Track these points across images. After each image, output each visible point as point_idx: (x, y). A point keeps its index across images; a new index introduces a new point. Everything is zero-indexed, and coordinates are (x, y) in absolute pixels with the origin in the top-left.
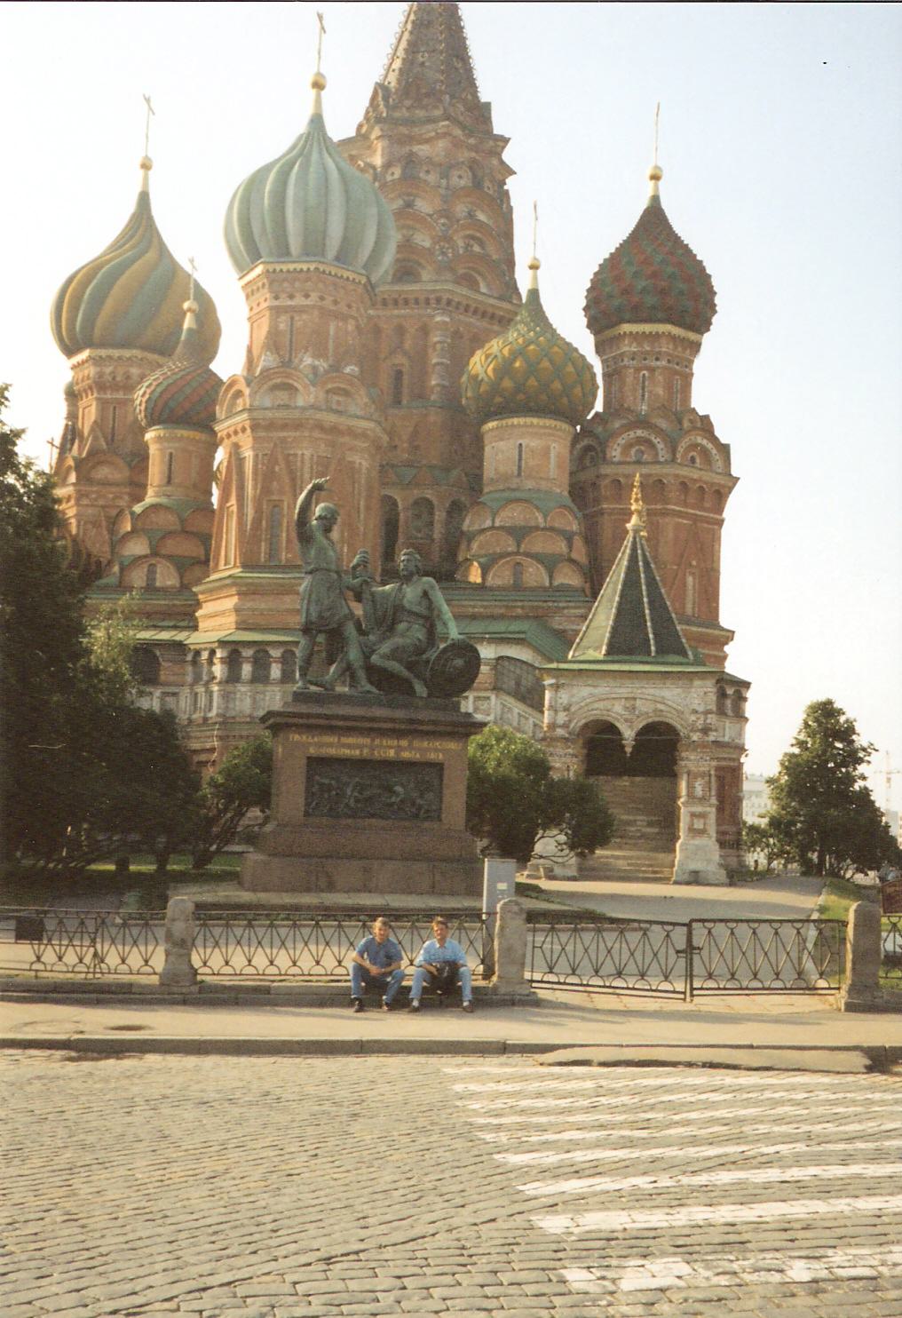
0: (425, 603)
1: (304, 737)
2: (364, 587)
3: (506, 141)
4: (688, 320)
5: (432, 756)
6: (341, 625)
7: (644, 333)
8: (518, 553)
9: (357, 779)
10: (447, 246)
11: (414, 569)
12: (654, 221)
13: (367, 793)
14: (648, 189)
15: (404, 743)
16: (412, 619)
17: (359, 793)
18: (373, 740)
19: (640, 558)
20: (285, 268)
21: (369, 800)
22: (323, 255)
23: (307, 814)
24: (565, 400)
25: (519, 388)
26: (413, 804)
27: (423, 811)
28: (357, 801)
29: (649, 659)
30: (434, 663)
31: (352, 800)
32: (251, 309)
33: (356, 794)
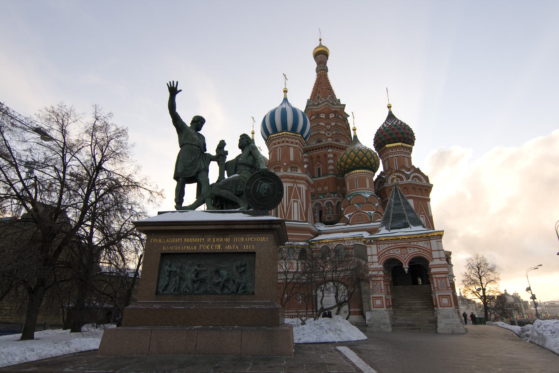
1: (160, 240)
2: (221, 158)
3: (345, 105)
4: (406, 141)
5: (246, 248)
6: (198, 172)
8: (359, 211)
9: (196, 267)
11: (246, 143)
14: (387, 111)
15: (227, 240)
17: (196, 276)
18: (206, 239)
20: (276, 135)
21: (203, 281)
24: (368, 163)
25: (353, 161)
26: (234, 282)
28: (194, 282)
30: (247, 184)
31: (190, 282)
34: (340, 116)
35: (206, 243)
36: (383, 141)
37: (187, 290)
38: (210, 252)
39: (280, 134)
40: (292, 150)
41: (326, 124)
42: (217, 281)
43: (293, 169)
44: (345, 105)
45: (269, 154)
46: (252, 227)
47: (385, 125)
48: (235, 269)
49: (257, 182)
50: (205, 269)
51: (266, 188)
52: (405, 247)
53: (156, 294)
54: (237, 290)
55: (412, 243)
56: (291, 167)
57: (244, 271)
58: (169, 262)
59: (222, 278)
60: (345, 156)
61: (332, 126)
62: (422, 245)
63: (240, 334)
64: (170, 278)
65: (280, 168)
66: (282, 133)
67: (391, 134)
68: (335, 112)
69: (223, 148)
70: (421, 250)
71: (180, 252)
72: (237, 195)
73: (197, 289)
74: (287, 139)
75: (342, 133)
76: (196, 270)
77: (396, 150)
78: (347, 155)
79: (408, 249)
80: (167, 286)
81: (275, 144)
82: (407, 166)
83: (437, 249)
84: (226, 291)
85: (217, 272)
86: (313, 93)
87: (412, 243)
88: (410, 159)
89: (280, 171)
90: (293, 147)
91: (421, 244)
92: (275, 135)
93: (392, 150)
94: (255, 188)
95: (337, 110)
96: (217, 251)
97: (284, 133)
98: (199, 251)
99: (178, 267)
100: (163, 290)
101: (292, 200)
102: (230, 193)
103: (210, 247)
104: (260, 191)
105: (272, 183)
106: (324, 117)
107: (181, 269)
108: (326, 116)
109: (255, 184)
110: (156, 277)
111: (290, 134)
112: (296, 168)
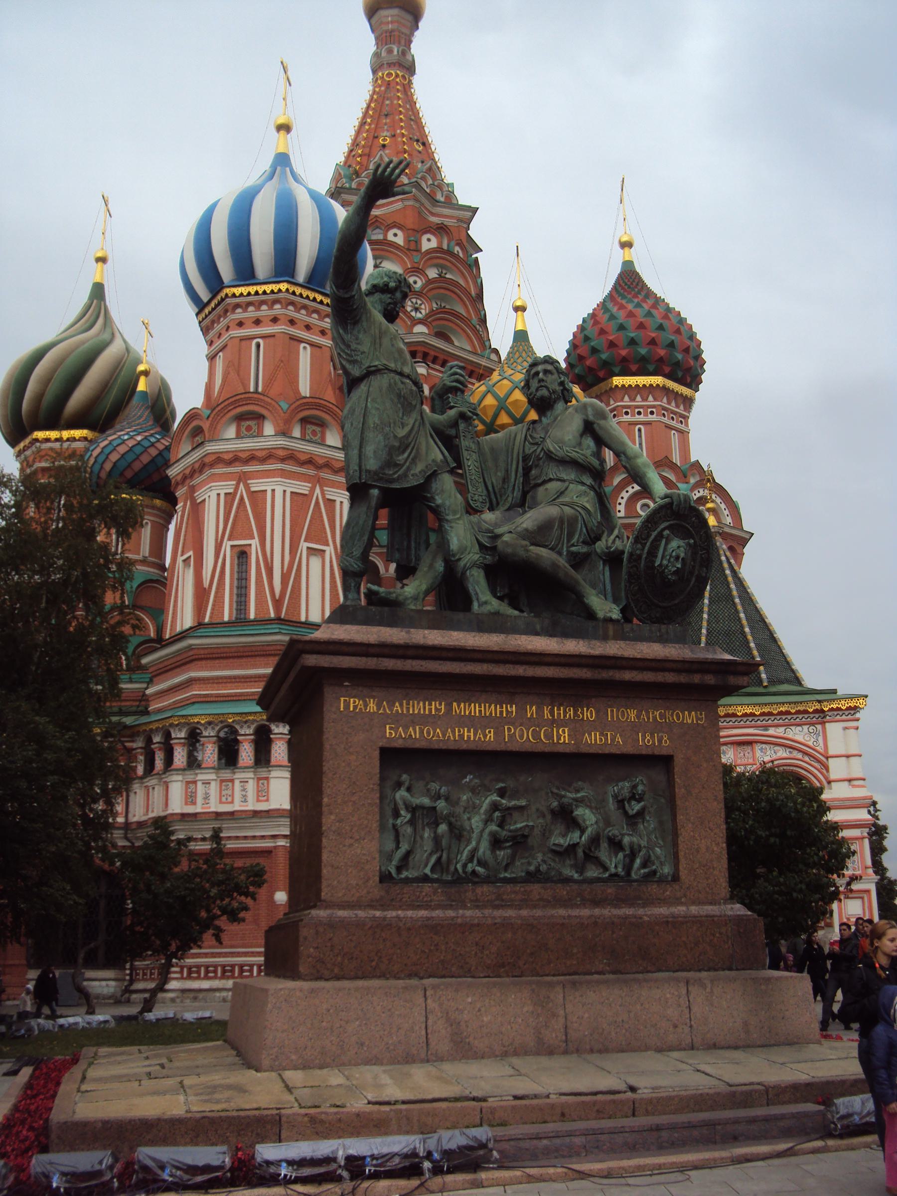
0: (589, 442)
1: (372, 706)
2: (462, 426)
3: (475, 210)
4: (680, 374)
5: (646, 742)
6: (432, 477)
7: (637, 386)
10: (419, 302)
11: (559, 389)
12: (629, 283)
13: (519, 824)
14: (618, 258)
15: (589, 714)
16: (569, 474)
17: (501, 825)
18: (522, 710)
19: (726, 565)
20: (252, 289)
21: (520, 841)
22: (293, 277)
23: (385, 878)
26: (616, 845)
27: (638, 861)
28: (496, 843)
29: (761, 690)
30: (637, 540)
32: (211, 343)
33: (493, 827)
34: (457, 249)
35: (520, 720)
36: (606, 364)
37: (479, 869)
38: (540, 748)
39: (268, 288)
40: (305, 356)
41: (406, 270)
42: (564, 842)
43: (310, 428)
44: (475, 210)
45: (212, 358)
46: (670, 678)
47: (614, 310)
48: (611, 805)
49: (660, 536)
50: (523, 803)
51: (682, 555)
52: (750, 743)
53: (381, 881)
54: (628, 869)
55: (771, 731)
56: (304, 421)
57: (641, 814)
58: (405, 777)
59: (583, 831)
60: (490, 401)
61: (430, 282)
62: (799, 738)
63: (684, 991)
64: (415, 830)
65: (260, 418)
66: (275, 287)
67: (633, 342)
68: (440, 230)
69: (463, 392)
70: (796, 754)
71: (442, 746)
72: (571, 566)
73: (506, 868)
74: (291, 311)
75: (461, 310)
76: (495, 807)
77: (645, 399)
78: (496, 396)
79: (757, 747)
80: (408, 854)
81: (240, 324)
82: (676, 459)
83: (843, 752)
84: (592, 872)
85: (565, 816)
86: (355, 144)
87: (771, 731)
88: (684, 434)
89: (260, 434)
90: (312, 345)
91: (800, 734)
92: (244, 290)
93: (633, 399)
94: (653, 553)
95: (448, 222)
96: (561, 749)
97: (284, 286)
98: (502, 747)
99: (437, 797)
100: (399, 869)
101: (304, 545)
102: (561, 560)
103: (536, 735)
104: (665, 562)
105: (692, 541)
106: (400, 240)
107: (447, 799)
108: (407, 240)
109: (655, 540)
110: (375, 825)
111: (305, 293)
112: (322, 425)
